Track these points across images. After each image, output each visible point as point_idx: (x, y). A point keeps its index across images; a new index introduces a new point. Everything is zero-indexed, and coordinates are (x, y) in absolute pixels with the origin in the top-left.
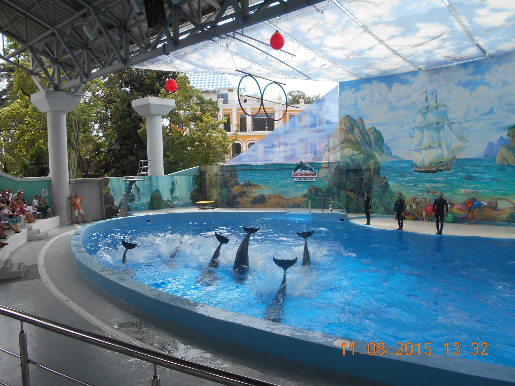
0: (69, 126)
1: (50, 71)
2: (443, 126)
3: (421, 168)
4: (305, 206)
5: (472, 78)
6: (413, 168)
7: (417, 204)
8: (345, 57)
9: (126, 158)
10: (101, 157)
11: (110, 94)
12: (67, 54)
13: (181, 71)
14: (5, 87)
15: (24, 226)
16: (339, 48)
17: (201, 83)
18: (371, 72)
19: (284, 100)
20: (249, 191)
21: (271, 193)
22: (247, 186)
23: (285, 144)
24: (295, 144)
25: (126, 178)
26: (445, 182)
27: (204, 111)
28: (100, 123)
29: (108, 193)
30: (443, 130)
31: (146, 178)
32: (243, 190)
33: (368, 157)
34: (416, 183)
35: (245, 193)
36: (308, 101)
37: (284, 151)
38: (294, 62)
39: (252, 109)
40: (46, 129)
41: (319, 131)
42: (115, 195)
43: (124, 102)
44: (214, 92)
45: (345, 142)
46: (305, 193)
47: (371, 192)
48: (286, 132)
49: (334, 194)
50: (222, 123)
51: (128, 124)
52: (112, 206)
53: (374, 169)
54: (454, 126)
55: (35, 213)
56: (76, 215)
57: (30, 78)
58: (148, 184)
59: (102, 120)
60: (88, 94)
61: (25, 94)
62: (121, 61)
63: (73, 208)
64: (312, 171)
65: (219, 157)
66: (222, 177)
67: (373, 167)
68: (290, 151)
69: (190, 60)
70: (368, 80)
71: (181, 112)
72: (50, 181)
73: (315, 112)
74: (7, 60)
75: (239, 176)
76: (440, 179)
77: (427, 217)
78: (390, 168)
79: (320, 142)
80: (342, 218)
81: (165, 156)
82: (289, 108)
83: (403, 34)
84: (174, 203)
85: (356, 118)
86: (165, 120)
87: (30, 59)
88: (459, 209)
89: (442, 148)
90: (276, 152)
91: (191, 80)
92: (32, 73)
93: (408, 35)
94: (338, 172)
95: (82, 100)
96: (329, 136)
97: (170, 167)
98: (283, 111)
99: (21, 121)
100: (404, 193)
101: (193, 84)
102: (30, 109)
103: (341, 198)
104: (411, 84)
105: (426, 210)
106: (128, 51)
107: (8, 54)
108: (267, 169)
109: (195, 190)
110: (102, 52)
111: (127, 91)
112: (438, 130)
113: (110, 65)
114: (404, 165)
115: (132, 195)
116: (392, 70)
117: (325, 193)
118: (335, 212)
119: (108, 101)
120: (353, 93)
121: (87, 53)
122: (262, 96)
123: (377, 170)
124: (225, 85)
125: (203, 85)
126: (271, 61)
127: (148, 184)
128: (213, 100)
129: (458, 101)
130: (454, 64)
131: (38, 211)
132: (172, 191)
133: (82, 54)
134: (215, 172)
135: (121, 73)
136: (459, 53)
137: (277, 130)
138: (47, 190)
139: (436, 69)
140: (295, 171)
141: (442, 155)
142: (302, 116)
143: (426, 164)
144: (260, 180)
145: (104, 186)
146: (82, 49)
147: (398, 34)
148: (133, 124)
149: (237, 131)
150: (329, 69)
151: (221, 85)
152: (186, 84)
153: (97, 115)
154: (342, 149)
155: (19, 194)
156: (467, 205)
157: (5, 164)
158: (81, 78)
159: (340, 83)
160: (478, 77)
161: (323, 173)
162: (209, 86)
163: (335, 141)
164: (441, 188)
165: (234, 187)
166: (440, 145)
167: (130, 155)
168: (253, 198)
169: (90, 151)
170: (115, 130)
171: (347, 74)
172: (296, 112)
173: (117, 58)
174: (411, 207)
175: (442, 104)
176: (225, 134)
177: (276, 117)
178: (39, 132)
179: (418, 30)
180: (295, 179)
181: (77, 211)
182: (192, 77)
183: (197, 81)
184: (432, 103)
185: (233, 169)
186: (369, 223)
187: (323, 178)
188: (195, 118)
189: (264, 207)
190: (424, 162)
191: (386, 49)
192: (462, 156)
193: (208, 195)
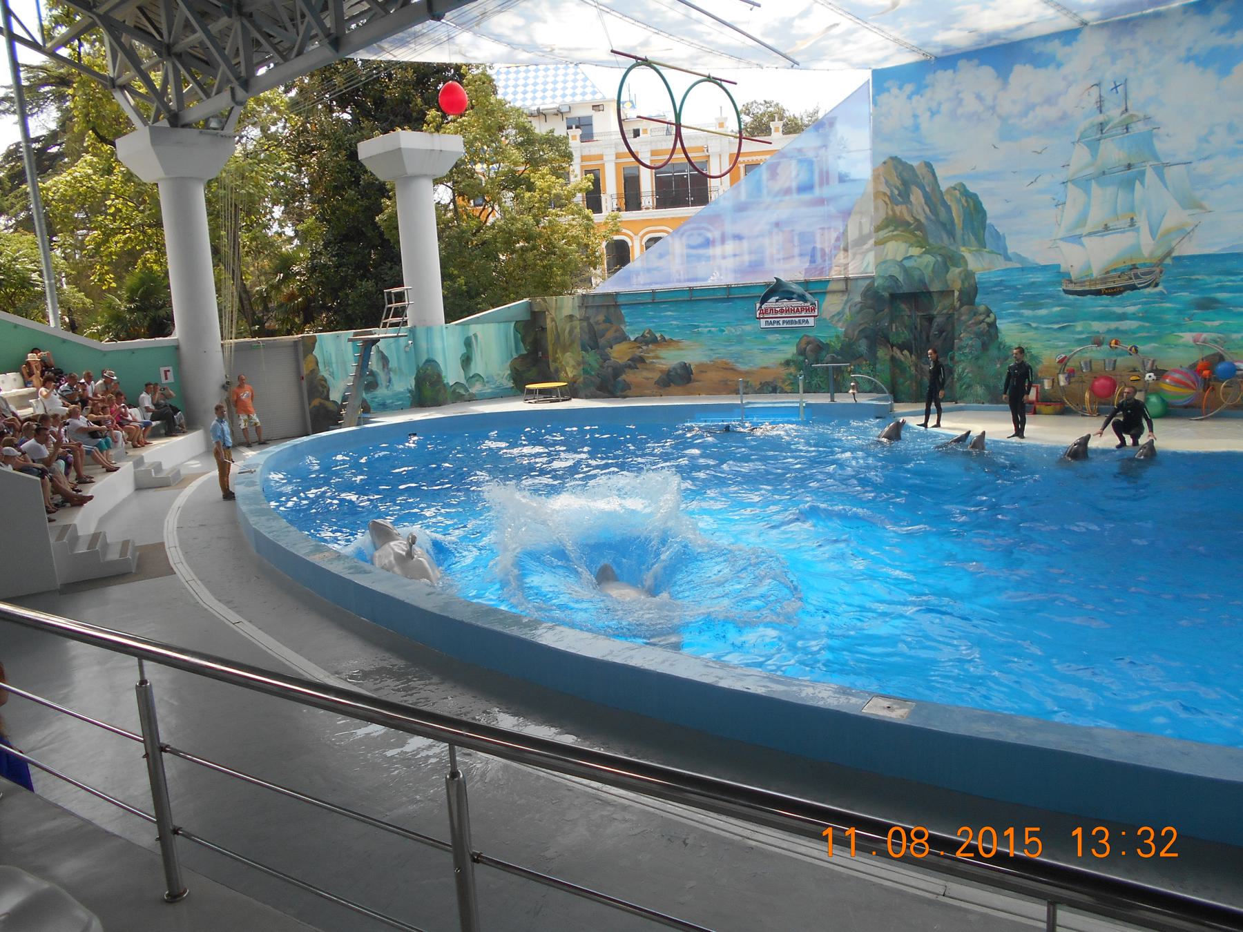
0: (213, 215)
1: (157, 77)
2: (1142, 173)
3: (1082, 283)
4: (788, 388)
6: (1060, 284)
7: (1071, 374)
9: (353, 287)
10: (293, 287)
11: (305, 130)
12: (194, 31)
13: (472, 62)
14: (53, 126)
15: (124, 457)
17: (525, 93)
18: (956, 37)
19: (733, 126)
20: (652, 354)
21: (705, 360)
22: (647, 344)
23: (738, 237)
25: (356, 334)
26: (1144, 317)
27: (533, 162)
28: (287, 204)
29: (314, 372)
30: (1142, 183)
31: (403, 331)
32: (638, 352)
33: (945, 263)
34: (1065, 323)
35: (642, 360)
37: (735, 255)
39: (654, 153)
40: (159, 224)
41: (821, 201)
42: (332, 374)
43: (340, 147)
44: (559, 113)
45: (887, 226)
46: (789, 356)
47: (952, 348)
48: (741, 208)
49: (861, 356)
50: (581, 190)
51: (352, 202)
52: (326, 403)
53: (961, 291)
54: (1172, 173)
55: (147, 425)
56: (243, 426)
57: (110, 100)
58: (407, 346)
59: (290, 197)
60: (254, 132)
61: (103, 140)
62: (326, 41)
63: (234, 409)
64: (806, 301)
65: (576, 276)
66: (585, 324)
67: (957, 286)
68: (750, 253)
69: (498, 30)
70: (948, 60)
71: (479, 167)
72: (177, 348)
74: (52, 54)
75: (627, 319)
76: (1131, 309)
77: (1095, 407)
78: (1004, 288)
79: (823, 229)
81: (445, 276)
82: (748, 146)
84: (473, 390)
85: (915, 164)
86: (441, 188)
87: (106, 49)
88: (1178, 383)
90: (714, 256)
91: (500, 84)
92: (112, 84)
94: (870, 302)
95: (239, 147)
96: (846, 214)
97: (459, 304)
98: (731, 155)
99: (96, 207)
100: (1036, 348)
101: (505, 94)
102: (117, 177)
103: (878, 366)
104: (1059, 65)
105: (1092, 389)
106: (343, 13)
107: (52, 38)
108: (693, 299)
109: (522, 357)
110: (277, 22)
111: (345, 121)
112: (1129, 185)
113: (299, 53)
114: (1038, 278)
115: (372, 373)
116: (1010, 31)
117: (838, 354)
118: (864, 399)
119: (301, 149)
120: (909, 97)
121: (243, 25)
122: (678, 116)
123: (970, 294)
124: (584, 94)
125: (529, 95)
126: (699, 22)
127: (407, 346)
128: (556, 134)
131: (153, 419)
132: (466, 361)
133: (229, 28)
134: (567, 311)
135: (327, 74)
137: (716, 202)
138: (170, 368)
140: (762, 303)
141: (1137, 248)
142: (778, 164)
143: (1096, 272)
144: (678, 327)
145: (305, 356)
146: (230, 16)
148: (365, 202)
149: (619, 210)
150: (845, 38)
151: (574, 95)
152: (487, 96)
153: (276, 185)
155: (108, 381)
156: (1199, 372)
157: (69, 312)
158: (232, 90)
159: (875, 72)
161: (832, 305)
162: (544, 98)
163: (862, 224)
164: (1133, 332)
165: (616, 347)
167: (362, 277)
168: (662, 371)
169: (265, 274)
170: (322, 219)
172: (763, 157)
173: (316, 36)
174: (1055, 382)
175: (1141, 115)
176: (589, 219)
177: (714, 170)
178: (144, 232)
180: (763, 321)
181: (243, 417)
182: (503, 77)
183: (516, 86)
185: (611, 303)
187: (833, 318)
188: (515, 182)
189: (689, 393)
190: (1090, 267)
192: (1189, 248)
193: (552, 369)
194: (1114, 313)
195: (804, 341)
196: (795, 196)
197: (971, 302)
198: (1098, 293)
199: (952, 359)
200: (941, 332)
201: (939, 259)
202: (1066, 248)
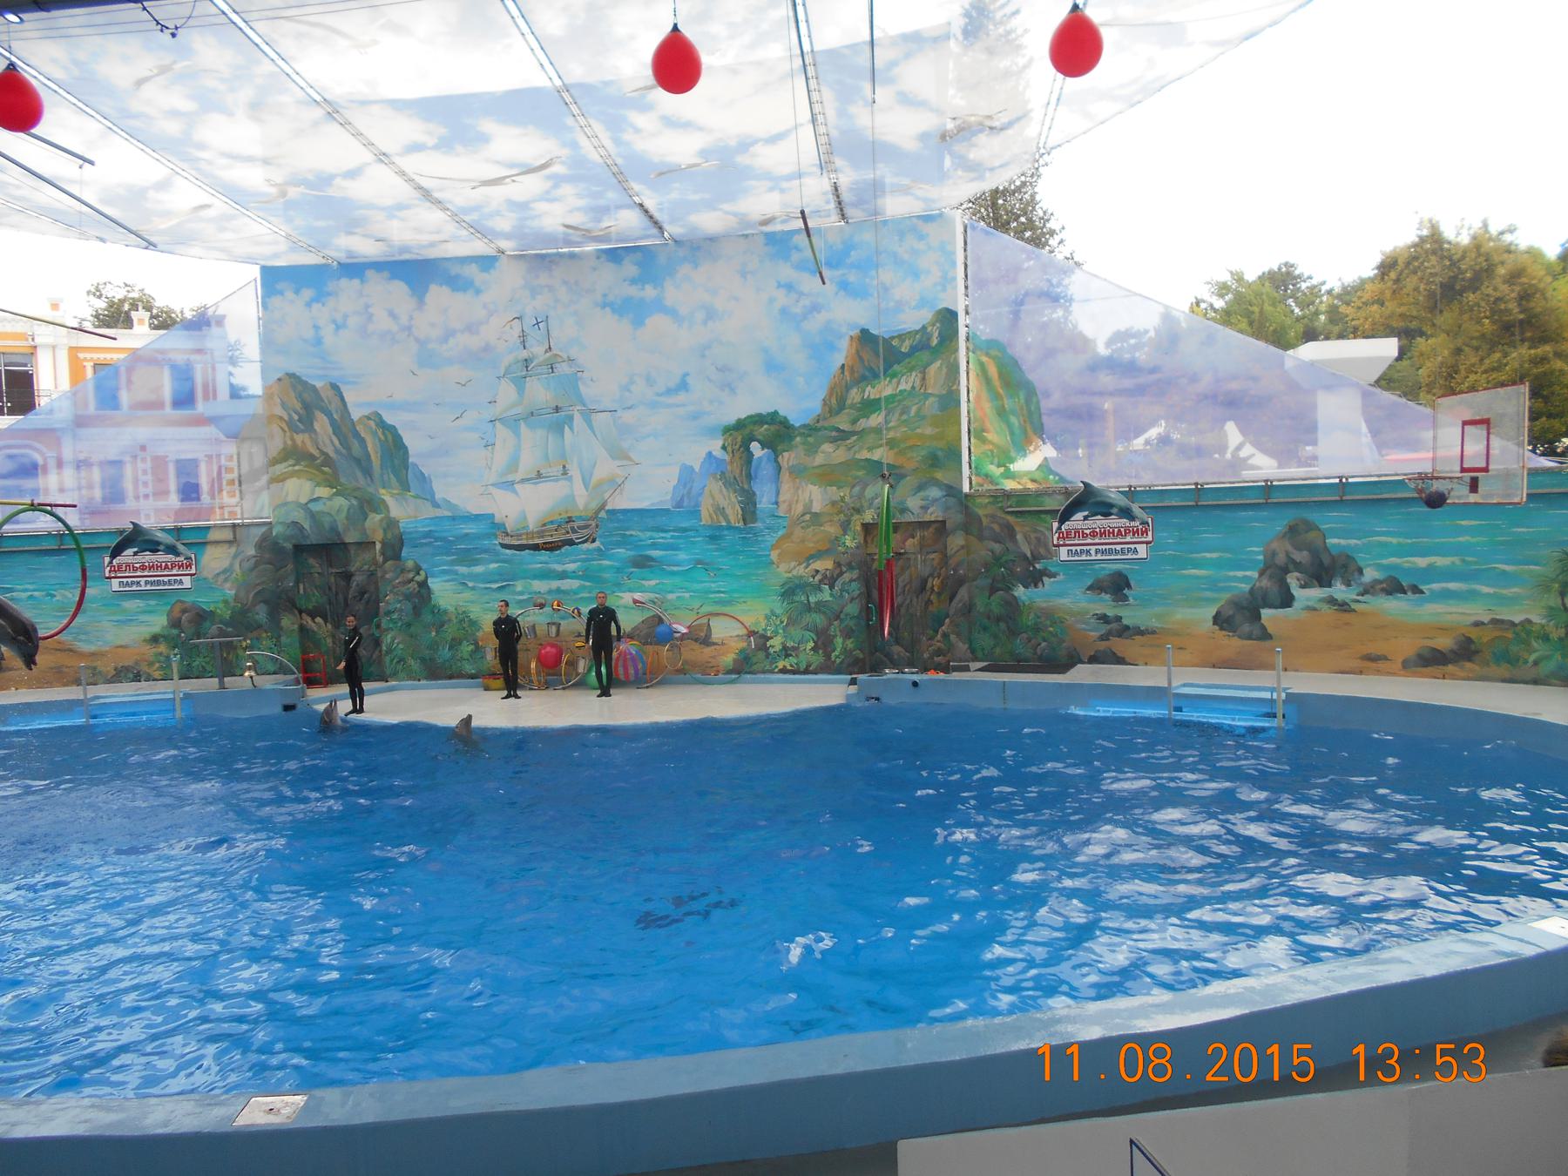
2: (571, 418)
5: (633, 291)
6: (496, 536)
8: (273, 190)
16: (250, 159)
23: (80, 465)
24: (117, 464)
30: (571, 428)
33: (362, 507)
34: (506, 579)
36: (163, 322)
38: (91, 185)
45: (285, 459)
46: (156, 629)
47: (377, 614)
49: (260, 626)
53: (383, 543)
54: (599, 419)
64: (178, 554)
67: (378, 536)
68: (103, 487)
70: (354, 269)
73: (180, 358)
76: (571, 567)
79: (210, 457)
80: (289, 702)
83: (444, 145)
85: (319, 384)
89: (570, 479)
93: (459, 148)
94: (267, 556)
100: (475, 612)
103: (283, 639)
104: (478, 292)
105: (541, 661)
112: (558, 429)
114: (471, 529)
116: (424, 247)
117: (227, 624)
120: (309, 305)
123: (394, 548)
129: (606, 353)
130: (590, 248)
136: (599, 221)
137: (51, 411)
139: (544, 260)
140: (114, 555)
143: (532, 525)
147: (431, 142)
154: (280, 479)
160: (649, 292)
161: (214, 560)
163: (256, 455)
166: (565, 473)
171: (283, 246)
179: (484, 139)
180: (115, 582)
184: (537, 350)
186: (358, 709)
187: (218, 576)
191: (399, 181)
192: (620, 502)
194: (554, 571)
195: (178, 608)
196: (168, 409)
197: (397, 557)
198: (536, 547)
199: (378, 626)
200: (363, 593)
201: (355, 502)
202: (499, 494)
